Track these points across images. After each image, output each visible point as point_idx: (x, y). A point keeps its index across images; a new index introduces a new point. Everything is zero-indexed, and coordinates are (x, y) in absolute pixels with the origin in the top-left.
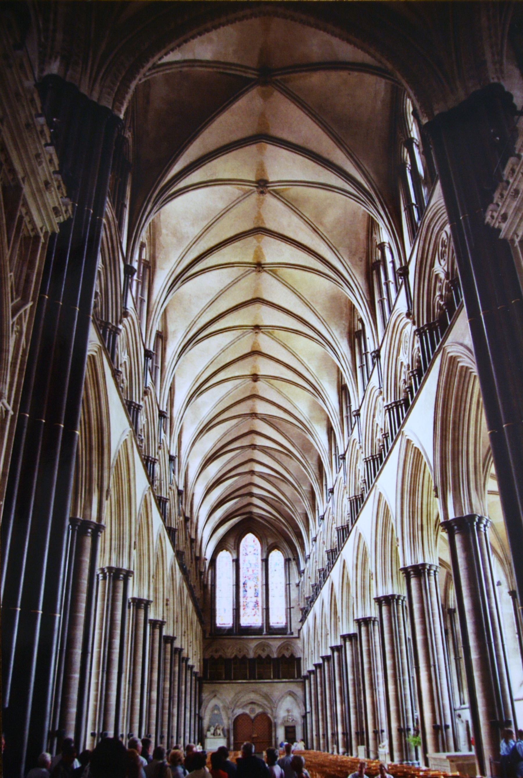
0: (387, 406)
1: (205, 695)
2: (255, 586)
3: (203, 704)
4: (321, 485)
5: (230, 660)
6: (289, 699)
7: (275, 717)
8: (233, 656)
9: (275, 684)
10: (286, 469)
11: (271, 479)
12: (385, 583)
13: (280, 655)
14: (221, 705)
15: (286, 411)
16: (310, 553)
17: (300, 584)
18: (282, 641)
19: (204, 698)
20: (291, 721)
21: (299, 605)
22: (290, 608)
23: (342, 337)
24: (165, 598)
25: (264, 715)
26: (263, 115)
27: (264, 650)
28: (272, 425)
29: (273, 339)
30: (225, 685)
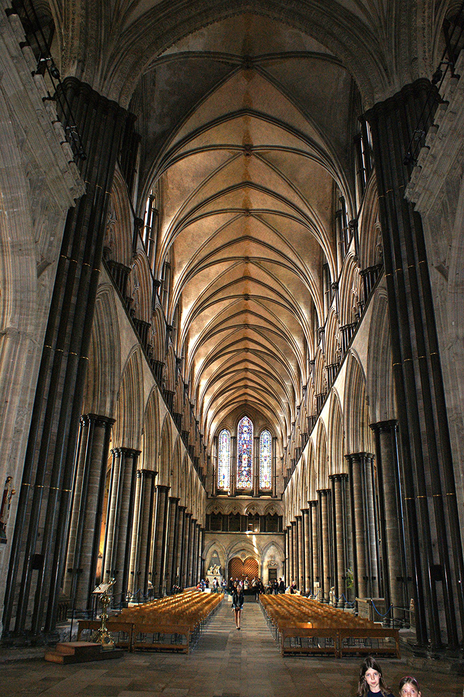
0: (342, 328)
1: (206, 542)
3: (205, 549)
5: (227, 515)
8: (230, 512)
10: (272, 368)
11: (261, 375)
12: (337, 464)
13: (267, 514)
14: (219, 550)
15: (271, 323)
17: (284, 458)
18: (268, 503)
23: (313, 269)
26: (247, 93)
27: (253, 509)
28: (260, 334)
30: (222, 535)
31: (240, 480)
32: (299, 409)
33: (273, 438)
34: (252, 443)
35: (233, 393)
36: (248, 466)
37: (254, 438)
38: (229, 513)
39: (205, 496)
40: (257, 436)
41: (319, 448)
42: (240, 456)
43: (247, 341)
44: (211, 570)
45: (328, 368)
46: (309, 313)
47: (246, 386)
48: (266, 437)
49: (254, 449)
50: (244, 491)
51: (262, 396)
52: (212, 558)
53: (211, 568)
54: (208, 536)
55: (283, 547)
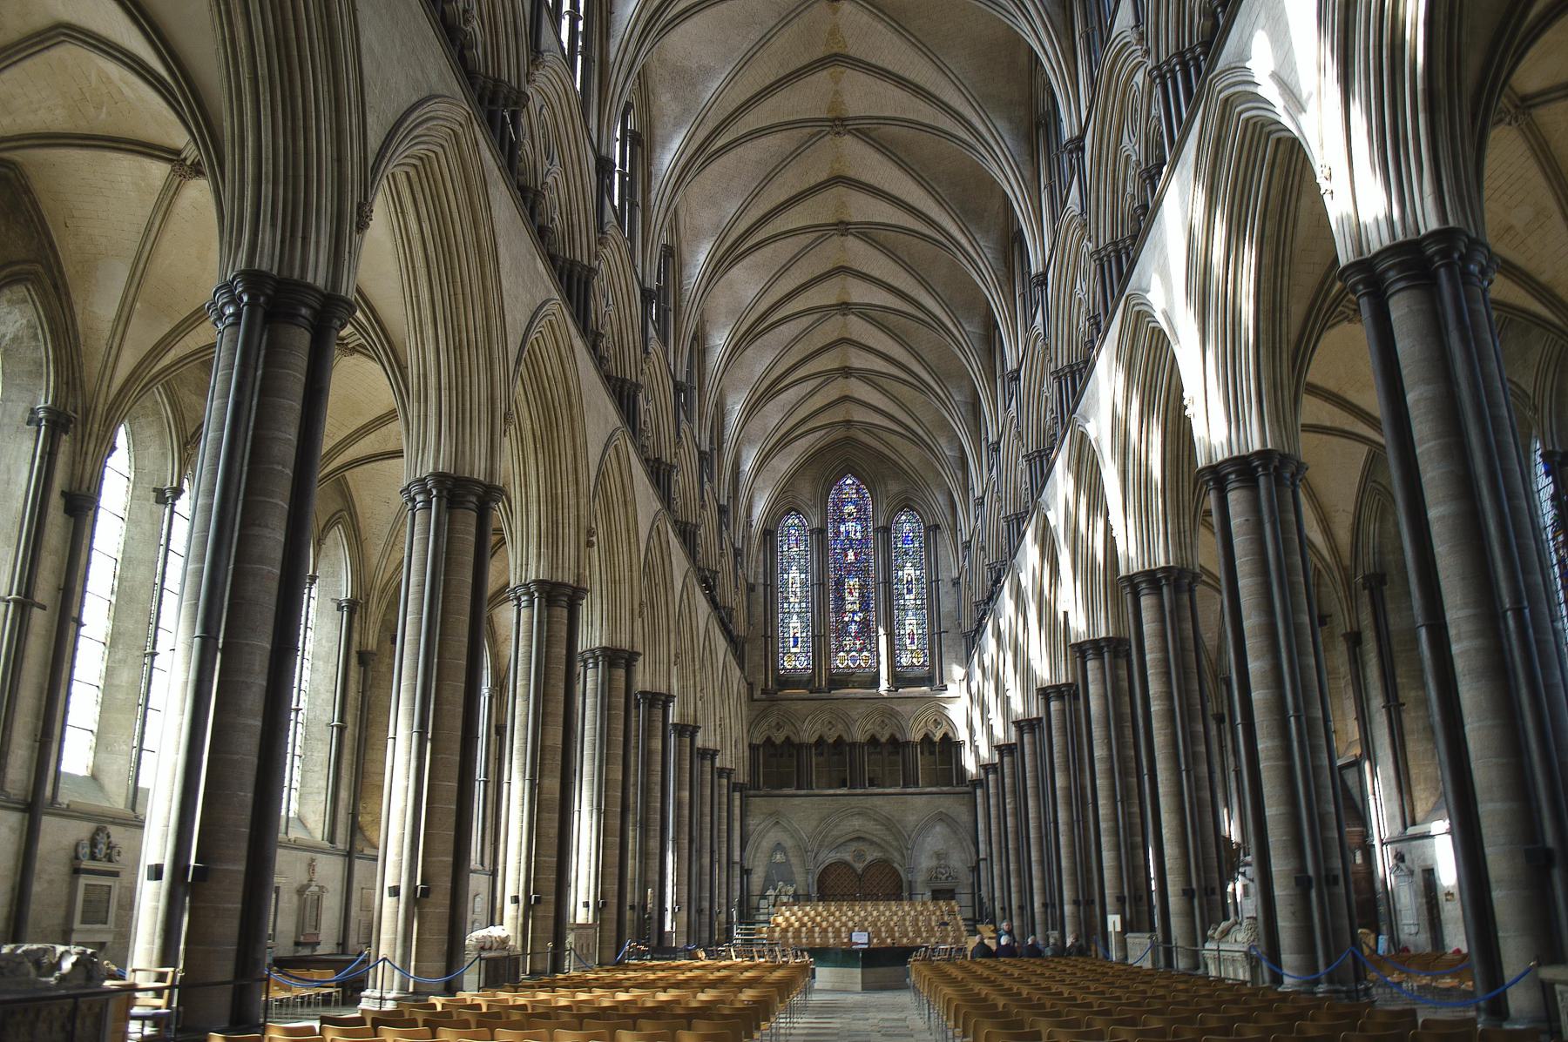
1: (752, 822)
2: (861, 587)
3: (751, 842)
5: (809, 746)
6: (939, 829)
7: (911, 870)
14: (788, 843)
16: (984, 492)
19: (751, 828)
20: (944, 877)
21: (960, 624)
22: (940, 633)
28: (883, 147)
30: (797, 801)
31: (841, 648)
32: (998, 450)
33: (928, 529)
36: (861, 611)
37: (876, 530)
38: (813, 740)
39: (744, 691)
42: (840, 584)
43: (840, 190)
44: (772, 899)
45: (1058, 375)
47: (846, 372)
48: (907, 527)
52: (772, 865)
54: (757, 803)
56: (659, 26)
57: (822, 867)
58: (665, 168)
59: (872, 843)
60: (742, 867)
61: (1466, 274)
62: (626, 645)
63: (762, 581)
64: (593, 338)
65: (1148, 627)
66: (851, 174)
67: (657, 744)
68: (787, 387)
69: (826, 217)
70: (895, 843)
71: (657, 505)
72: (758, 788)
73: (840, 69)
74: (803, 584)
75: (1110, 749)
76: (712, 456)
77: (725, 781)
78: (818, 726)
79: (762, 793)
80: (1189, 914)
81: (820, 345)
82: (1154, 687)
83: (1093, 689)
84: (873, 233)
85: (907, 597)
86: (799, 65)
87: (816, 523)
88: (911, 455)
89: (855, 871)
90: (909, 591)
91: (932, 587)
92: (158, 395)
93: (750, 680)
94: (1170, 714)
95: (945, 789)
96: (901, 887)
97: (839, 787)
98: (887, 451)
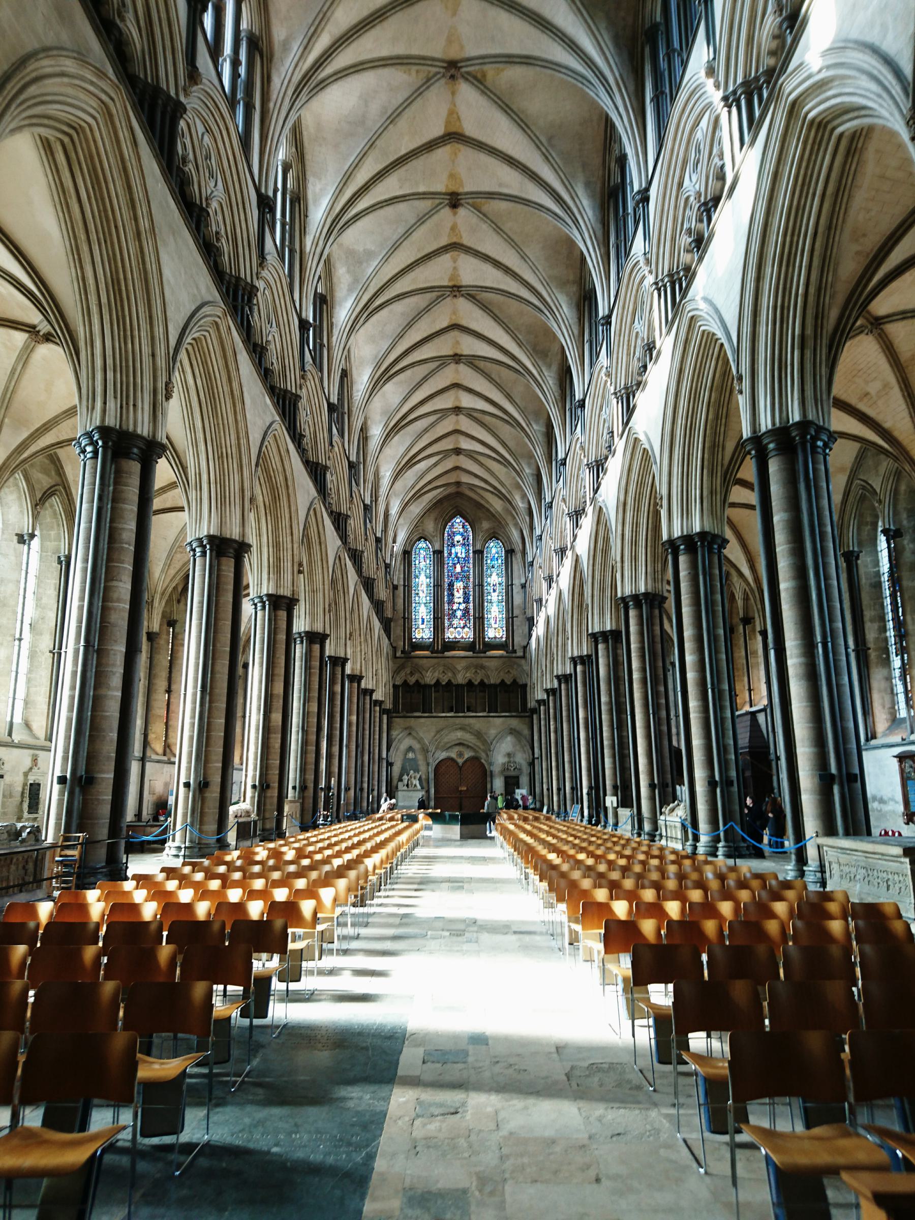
1: (394, 733)
2: (465, 588)
4: (562, 412)
5: (430, 686)
6: (509, 739)
7: (491, 764)
9: (491, 719)
11: (487, 419)
13: (498, 681)
14: (417, 746)
16: (542, 532)
17: (527, 585)
21: (525, 613)
22: (513, 618)
24: (296, 559)
25: (475, 760)
29: (483, 92)
30: (422, 720)
31: (451, 625)
33: (507, 552)
34: (471, 561)
35: (435, 465)
36: (464, 602)
38: (433, 682)
39: (390, 653)
40: (478, 547)
41: (625, 504)
42: (451, 585)
46: (574, 310)
47: (458, 451)
48: (494, 550)
49: (474, 572)
50: (459, 645)
51: (488, 470)
52: (405, 759)
53: (405, 778)
54: (398, 722)
55: (529, 737)
56: (339, 227)
57: (437, 762)
58: (342, 320)
59: (468, 747)
60: (387, 761)
61: (814, 447)
62: (320, 630)
63: (402, 583)
64: (297, 437)
65: (633, 628)
66: (464, 323)
67: (338, 688)
68: (419, 461)
69: (447, 351)
70: (482, 747)
71: (339, 543)
72: (398, 712)
73: (457, 253)
74: (428, 586)
75: (611, 697)
76: (371, 507)
77: (378, 708)
78: (436, 674)
79: (401, 715)
80: (652, 798)
81: (441, 434)
82: (635, 664)
83: (601, 661)
84: (477, 363)
85: (493, 594)
86: (430, 250)
87: (437, 547)
88: (497, 505)
89: (457, 764)
90: (494, 591)
91: (509, 586)
92: (19, 476)
93: (394, 645)
94: (644, 681)
95: (514, 714)
96: (486, 774)
97: (448, 712)
98: (483, 502)
